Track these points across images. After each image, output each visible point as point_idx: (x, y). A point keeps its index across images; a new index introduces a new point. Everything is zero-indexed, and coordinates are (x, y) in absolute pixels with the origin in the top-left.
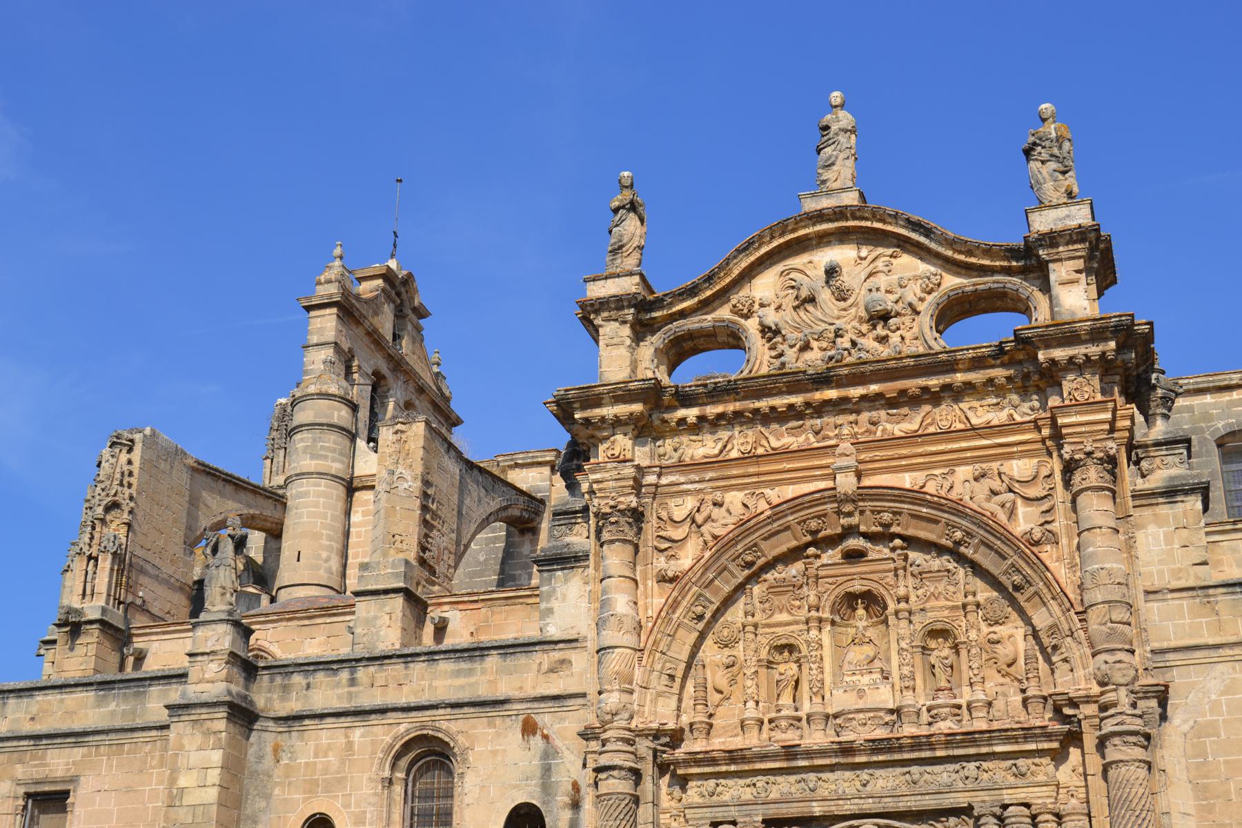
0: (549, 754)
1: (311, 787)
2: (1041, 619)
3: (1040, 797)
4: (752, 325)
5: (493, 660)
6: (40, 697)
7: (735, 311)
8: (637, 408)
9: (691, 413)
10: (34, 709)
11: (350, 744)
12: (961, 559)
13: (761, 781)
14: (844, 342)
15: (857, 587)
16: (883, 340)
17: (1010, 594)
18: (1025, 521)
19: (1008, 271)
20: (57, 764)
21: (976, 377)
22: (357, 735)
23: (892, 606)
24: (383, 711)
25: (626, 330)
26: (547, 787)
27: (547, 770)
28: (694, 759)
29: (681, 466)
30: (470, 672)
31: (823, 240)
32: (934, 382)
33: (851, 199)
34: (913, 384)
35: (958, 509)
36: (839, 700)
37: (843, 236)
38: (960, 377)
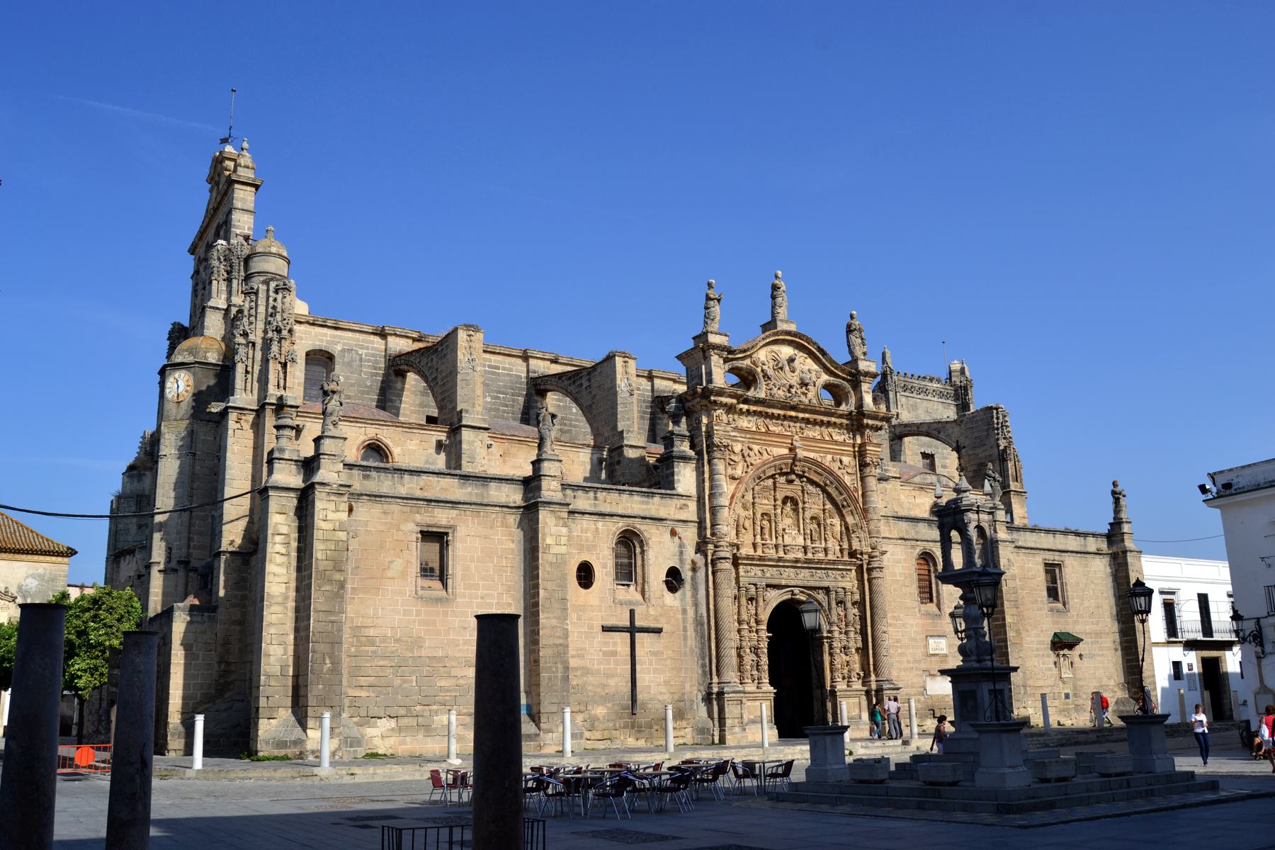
0: (681, 546)
1: (581, 548)
2: (850, 520)
3: (848, 585)
4: (759, 370)
5: (657, 499)
6: (424, 477)
7: (754, 363)
8: (735, 401)
9: (745, 407)
10: (422, 484)
11: (597, 529)
12: (824, 491)
13: (765, 569)
14: (793, 391)
15: (790, 494)
16: (805, 394)
17: (839, 509)
18: (847, 480)
19: (844, 379)
20: (442, 517)
21: (838, 421)
22: (600, 524)
23: (801, 505)
24: (612, 515)
25: (721, 361)
26: (682, 561)
27: (681, 553)
28: (748, 558)
29: (736, 429)
30: (647, 503)
31: (783, 342)
32: (825, 419)
33: (793, 327)
34: (819, 418)
35: (831, 473)
36: (788, 540)
37: (790, 343)
38: (833, 419)
